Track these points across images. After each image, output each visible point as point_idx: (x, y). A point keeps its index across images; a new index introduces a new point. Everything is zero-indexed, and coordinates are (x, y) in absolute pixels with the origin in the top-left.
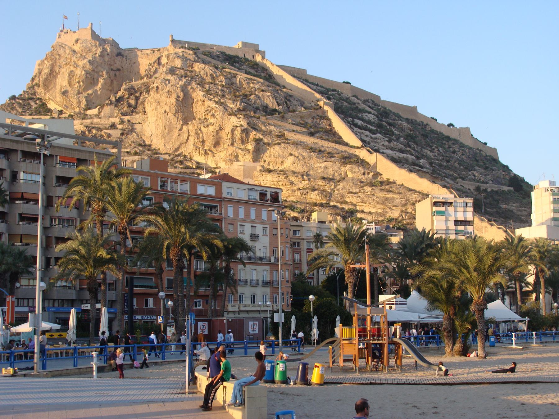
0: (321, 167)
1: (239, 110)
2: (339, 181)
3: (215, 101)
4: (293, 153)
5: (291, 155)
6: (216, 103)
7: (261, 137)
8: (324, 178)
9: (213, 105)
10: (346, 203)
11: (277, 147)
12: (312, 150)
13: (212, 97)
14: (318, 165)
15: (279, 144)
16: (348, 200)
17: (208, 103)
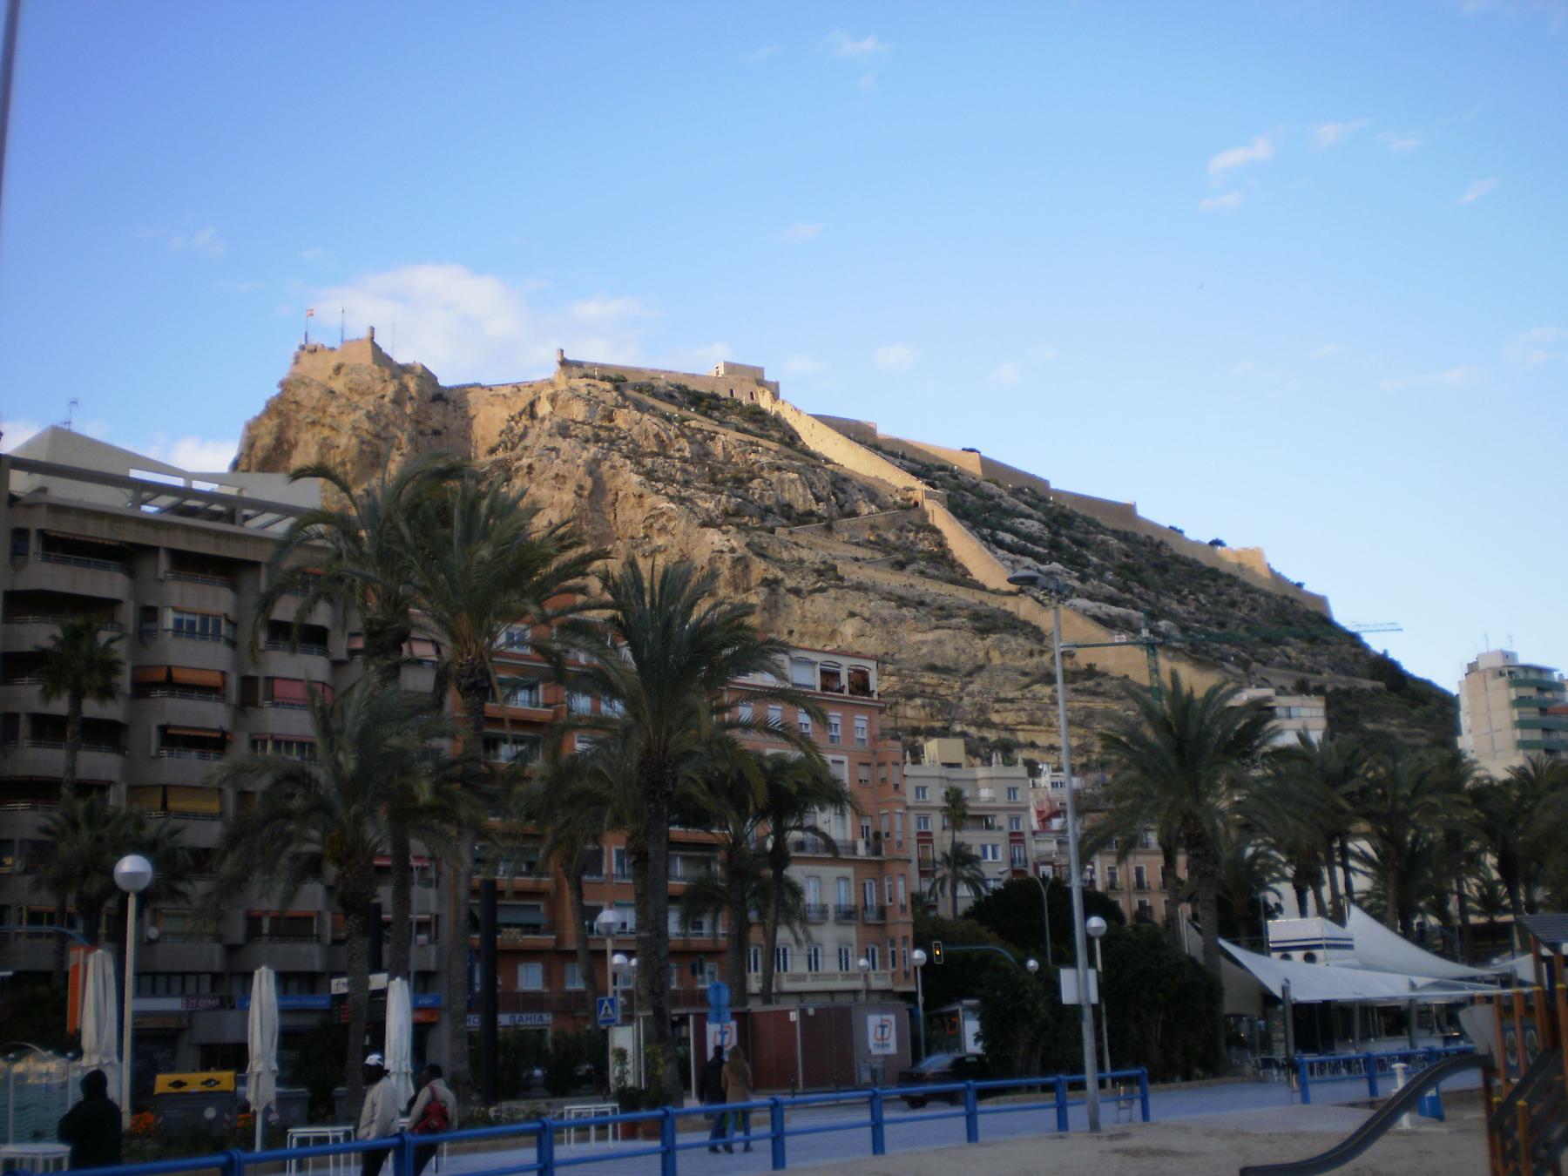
0: (924, 643)
1: (726, 513)
2: (970, 674)
3: (666, 494)
4: (857, 609)
5: (852, 615)
6: (671, 499)
7: (780, 574)
8: (933, 668)
9: (665, 505)
10: (989, 725)
11: (818, 597)
12: (902, 602)
13: (660, 485)
14: (919, 637)
15: (822, 590)
16: (995, 718)
17: (650, 500)
